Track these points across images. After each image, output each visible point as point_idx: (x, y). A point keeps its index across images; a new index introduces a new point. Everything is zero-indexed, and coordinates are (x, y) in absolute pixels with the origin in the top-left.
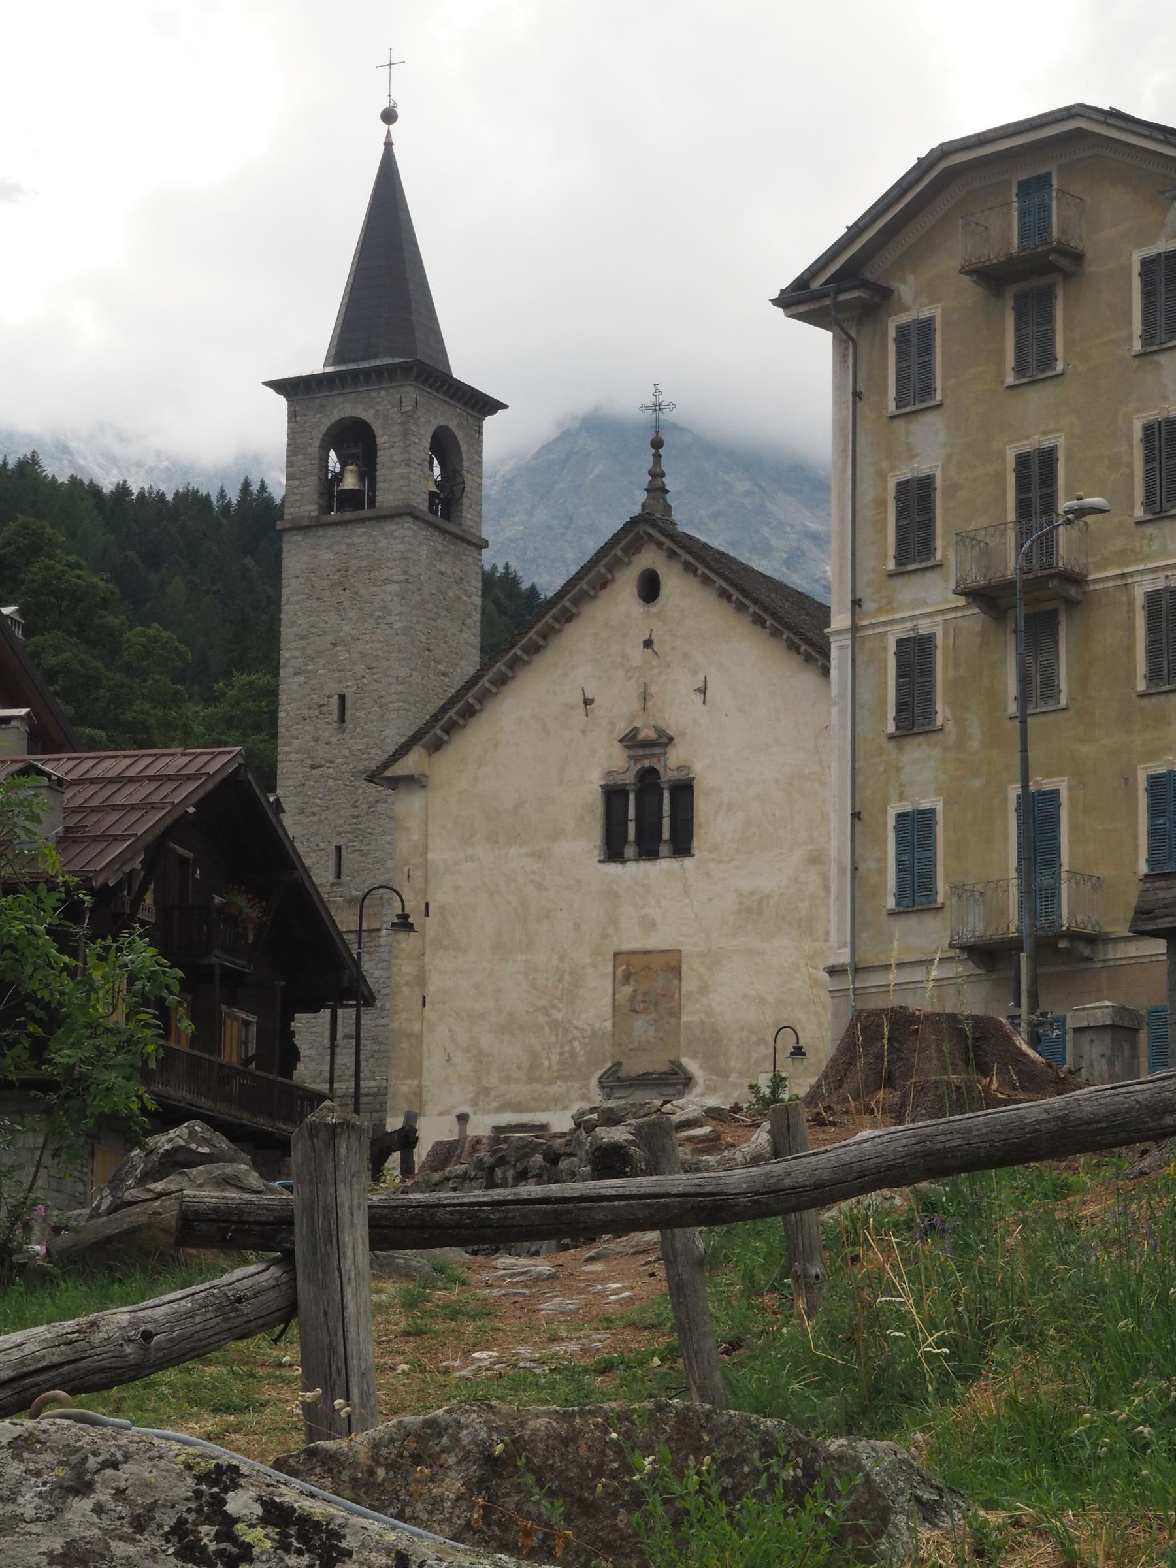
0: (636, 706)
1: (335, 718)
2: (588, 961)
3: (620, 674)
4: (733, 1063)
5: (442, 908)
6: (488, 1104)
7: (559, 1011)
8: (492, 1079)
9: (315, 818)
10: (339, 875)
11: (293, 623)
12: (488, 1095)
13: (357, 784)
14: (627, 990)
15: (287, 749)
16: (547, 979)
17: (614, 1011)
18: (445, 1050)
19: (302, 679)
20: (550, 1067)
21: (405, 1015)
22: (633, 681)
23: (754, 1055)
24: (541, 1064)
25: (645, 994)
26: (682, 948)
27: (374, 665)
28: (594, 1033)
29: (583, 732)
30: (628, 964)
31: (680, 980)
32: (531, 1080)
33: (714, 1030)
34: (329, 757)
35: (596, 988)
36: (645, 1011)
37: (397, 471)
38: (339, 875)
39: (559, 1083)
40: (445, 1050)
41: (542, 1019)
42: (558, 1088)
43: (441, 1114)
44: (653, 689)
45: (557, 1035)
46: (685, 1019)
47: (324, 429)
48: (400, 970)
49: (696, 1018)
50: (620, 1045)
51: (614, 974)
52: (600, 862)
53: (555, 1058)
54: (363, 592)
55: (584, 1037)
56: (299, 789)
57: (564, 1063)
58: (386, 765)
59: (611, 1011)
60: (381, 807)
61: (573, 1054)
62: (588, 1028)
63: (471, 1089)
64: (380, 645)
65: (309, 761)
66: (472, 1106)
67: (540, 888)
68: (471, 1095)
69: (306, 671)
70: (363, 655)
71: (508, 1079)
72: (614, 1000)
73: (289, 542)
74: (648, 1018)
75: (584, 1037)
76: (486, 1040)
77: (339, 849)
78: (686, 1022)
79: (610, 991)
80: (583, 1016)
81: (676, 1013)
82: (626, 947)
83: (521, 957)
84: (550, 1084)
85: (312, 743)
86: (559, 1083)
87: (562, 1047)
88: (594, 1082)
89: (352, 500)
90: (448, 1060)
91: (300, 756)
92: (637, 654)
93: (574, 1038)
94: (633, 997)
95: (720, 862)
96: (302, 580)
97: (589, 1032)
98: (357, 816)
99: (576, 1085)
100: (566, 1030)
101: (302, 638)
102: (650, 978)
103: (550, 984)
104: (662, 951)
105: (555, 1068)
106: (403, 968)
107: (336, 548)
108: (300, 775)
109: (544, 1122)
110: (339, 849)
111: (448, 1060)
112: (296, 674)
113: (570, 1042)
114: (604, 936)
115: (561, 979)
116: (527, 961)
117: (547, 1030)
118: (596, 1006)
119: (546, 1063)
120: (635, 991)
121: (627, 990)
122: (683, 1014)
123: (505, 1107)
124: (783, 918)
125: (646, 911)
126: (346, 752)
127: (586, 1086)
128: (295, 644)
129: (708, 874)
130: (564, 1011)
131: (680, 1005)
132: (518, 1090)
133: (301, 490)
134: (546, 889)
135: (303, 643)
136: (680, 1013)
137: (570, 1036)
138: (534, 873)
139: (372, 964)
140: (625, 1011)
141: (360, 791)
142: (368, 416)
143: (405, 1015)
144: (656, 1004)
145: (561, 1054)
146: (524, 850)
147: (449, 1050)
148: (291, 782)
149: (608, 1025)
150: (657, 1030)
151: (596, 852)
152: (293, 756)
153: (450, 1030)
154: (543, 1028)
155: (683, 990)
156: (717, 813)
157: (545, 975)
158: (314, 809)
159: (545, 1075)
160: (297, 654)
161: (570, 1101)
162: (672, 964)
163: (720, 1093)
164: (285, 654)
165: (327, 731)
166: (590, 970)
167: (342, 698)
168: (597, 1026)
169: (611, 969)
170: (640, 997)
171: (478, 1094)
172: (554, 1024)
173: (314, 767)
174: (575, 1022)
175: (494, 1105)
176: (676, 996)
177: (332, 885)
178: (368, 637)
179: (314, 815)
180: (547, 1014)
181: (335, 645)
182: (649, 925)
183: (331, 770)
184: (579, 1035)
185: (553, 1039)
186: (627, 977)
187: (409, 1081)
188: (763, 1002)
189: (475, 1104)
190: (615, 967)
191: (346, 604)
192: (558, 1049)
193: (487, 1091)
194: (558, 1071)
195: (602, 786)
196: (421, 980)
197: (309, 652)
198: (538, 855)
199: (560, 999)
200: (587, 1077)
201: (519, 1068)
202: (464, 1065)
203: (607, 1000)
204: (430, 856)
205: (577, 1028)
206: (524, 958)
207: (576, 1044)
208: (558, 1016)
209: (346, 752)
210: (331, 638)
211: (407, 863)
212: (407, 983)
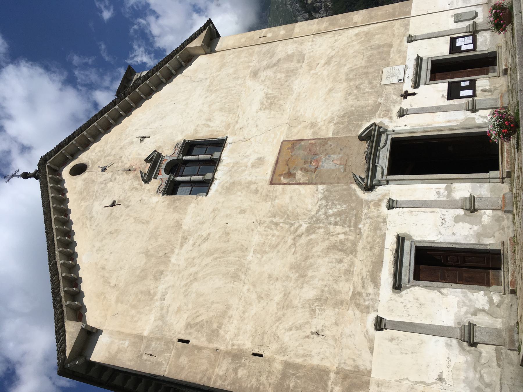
0: (132, 174)
2: (270, 203)
3: (110, 185)
4: (371, 102)
5: (189, 326)
6: (368, 295)
7: (300, 226)
8: (346, 289)
12: (360, 294)
14: (299, 175)
16: (273, 236)
17: (311, 184)
18: (307, 337)
20: (345, 233)
21: (263, 379)
22: (118, 177)
23: (367, 90)
24: (341, 240)
25: (305, 162)
26: (282, 140)
28: (326, 198)
29: (128, 207)
30: (280, 175)
31: (303, 140)
32: (353, 251)
33: (343, 116)
35: (291, 198)
36: (317, 162)
39: (360, 226)
40: (307, 337)
41: (303, 240)
42: (365, 227)
43: (372, 352)
44: (128, 166)
45: (319, 228)
46: (330, 135)
48: (221, 377)
49: (332, 127)
50: (339, 178)
51: (285, 184)
52: (206, 195)
53: (339, 229)
55: (326, 206)
57: (344, 222)
59: (311, 186)
61: (339, 214)
62: (320, 203)
63: (350, 312)
66: (368, 313)
67: (206, 239)
68: (357, 312)
71: (348, 272)
72: (304, 184)
74: (324, 159)
75: (326, 206)
76: (309, 293)
78: (333, 134)
79: (297, 186)
80: (310, 207)
81: (325, 141)
82: (268, 177)
83: (250, 257)
84: (360, 233)
86: (360, 226)
87: (330, 224)
88: (365, 196)
90: (317, 333)
92: (107, 175)
93: (326, 213)
94: (305, 170)
95: (237, 122)
97: (324, 202)
99: (366, 211)
100: (318, 220)
102: (296, 161)
103: (277, 233)
104: (279, 152)
105: (348, 229)
106: (221, 373)
109: (395, 240)
111: (317, 333)
113: (327, 216)
114: (256, 191)
115: (277, 224)
116: (254, 251)
117: (313, 236)
118: (305, 197)
119: (342, 237)
120: (301, 169)
121: (299, 175)
122: (327, 137)
123: (374, 278)
124: (282, 85)
125: (249, 164)
127: (368, 203)
129: (241, 129)
130: (301, 222)
131: (319, 139)
132: (361, 265)
134: (209, 234)
136: (325, 139)
137: (322, 216)
138: (194, 244)
140: (314, 176)
143: (263, 379)
144: (315, 154)
145: (336, 224)
146: (176, 251)
147: (308, 333)
149: (321, 187)
150: (334, 153)
151: (200, 197)
153: (290, 329)
154: (311, 239)
155: (311, 138)
156: (209, 126)
157: (269, 237)
159: (351, 238)
161: (378, 216)
162: (290, 145)
163: (392, 107)
166: (277, 201)
168: (320, 196)
169: (281, 187)
170: (306, 166)
171: (358, 305)
172: (310, 231)
174: (313, 213)
175: (370, 289)
176: (313, 142)
180: (300, 236)
182: (260, 161)
184: (323, 210)
185: (322, 231)
186: (290, 175)
187: (330, 383)
188: (331, 90)
189: (367, 309)
190: (280, 184)
192: (331, 227)
193: (356, 294)
194: (350, 227)
195: (163, 195)
196: (236, 356)
198: (185, 239)
199: (292, 225)
200: (361, 202)
201: (340, 261)
202: (325, 319)
203: (301, 188)
204: (146, 334)
205: (318, 211)
206: (251, 254)
207: (330, 212)
208: (305, 226)
211: (141, 355)
212: (236, 370)
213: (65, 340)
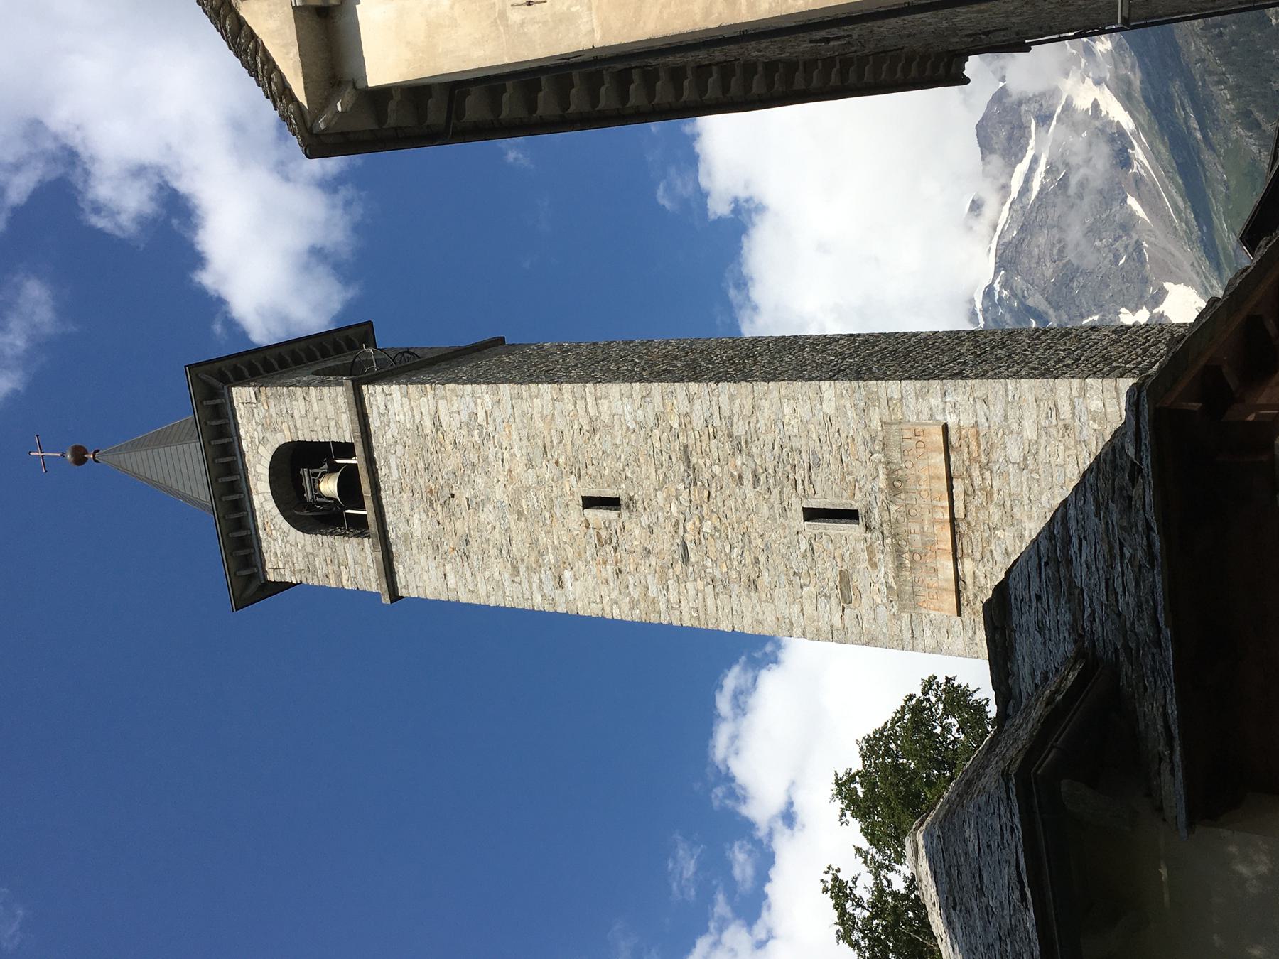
1: (612, 514)
9: (762, 560)
10: (850, 516)
11: (499, 585)
13: (707, 475)
15: (663, 607)
19: (567, 575)
27: (541, 444)
34: (669, 527)
37: (315, 408)
38: (850, 516)
47: (286, 525)
54: (453, 462)
56: (720, 588)
58: (279, 92)
60: (739, 429)
64: (514, 433)
65: (679, 567)
69: (557, 567)
70: (530, 465)
73: (406, 587)
77: (811, 515)
85: (653, 559)
89: (349, 482)
91: (671, 583)
96: (448, 567)
98: (755, 474)
101: (516, 570)
107: (407, 510)
108: (700, 585)
110: (811, 515)
112: (560, 583)
126: (661, 495)
128: (525, 585)
133: (351, 562)
135: (522, 569)
139: (1011, 442)
141: (716, 469)
142: (266, 455)
148: (710, 602)
152: (673, 596)
158: (749, 560)
160: (535, 578)
164: (538, 603)
165: (634, 529)
167: (590, 502)
173: (686, 558)
177: (868, 528)
178: (507, 456)
179: (757, 561)
181: (521, 514)
183: (689, 526)
191: (468, 493)
197: (532, 559)
209: (661, 495)
210: (511, 518)
211: (503, 15)
213: (268, 59)
